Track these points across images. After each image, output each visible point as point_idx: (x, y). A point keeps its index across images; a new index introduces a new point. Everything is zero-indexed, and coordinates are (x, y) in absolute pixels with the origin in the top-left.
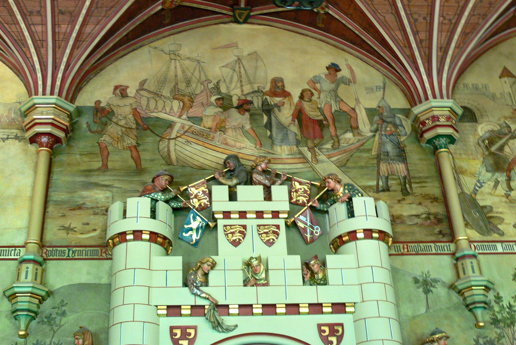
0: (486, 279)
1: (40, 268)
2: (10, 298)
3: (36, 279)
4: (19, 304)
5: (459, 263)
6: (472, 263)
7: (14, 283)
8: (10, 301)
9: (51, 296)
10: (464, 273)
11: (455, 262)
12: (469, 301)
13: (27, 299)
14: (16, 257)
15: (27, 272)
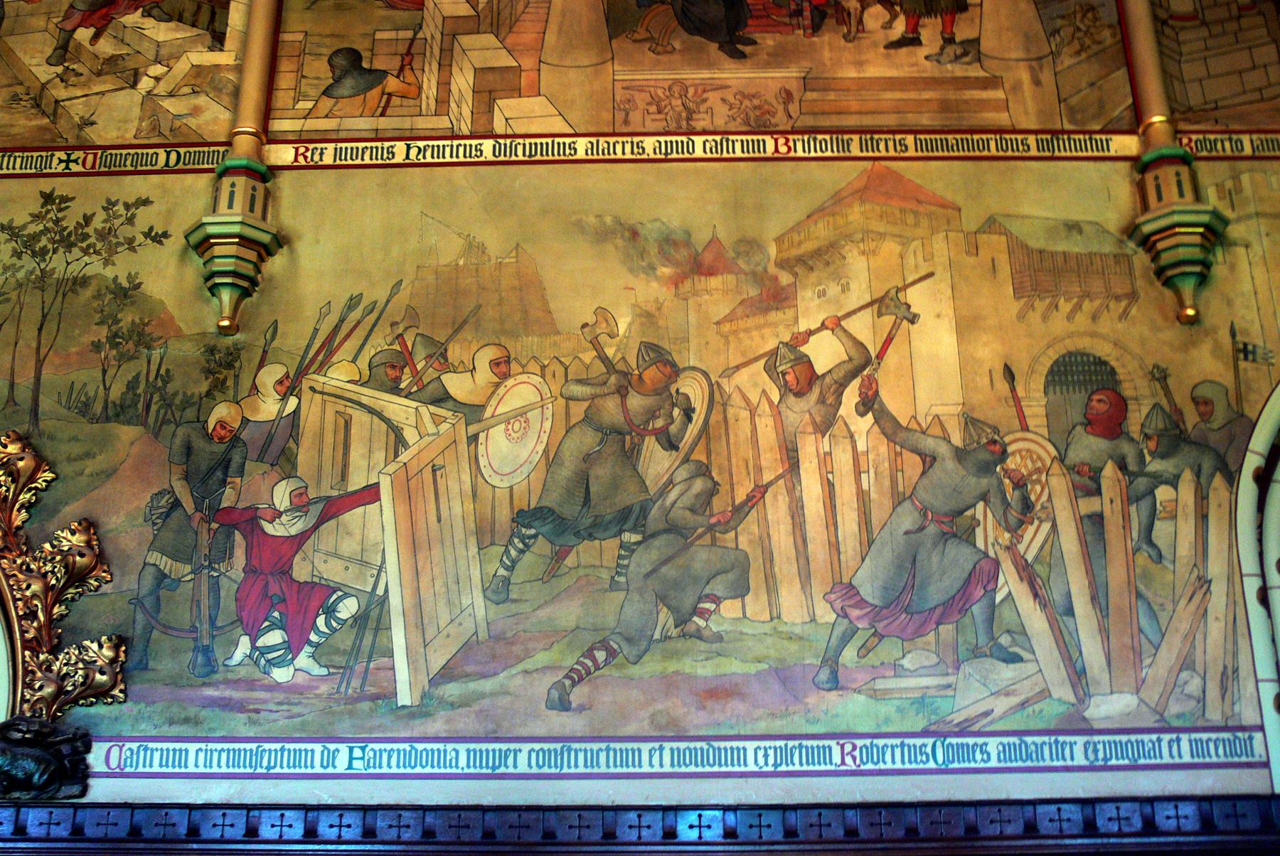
0: (1210, 208)
1: (260, 187)
2: (203, 248)
3: (252, 210)
4: (217, 260)
5: (1149, 177)
6: (1178, 174)
7: (206, 216)
8: (201, 255)
9: (285, 247)
10: (1160, 198)
11: (1138, 177)
12: (1166, 258)
13: (232, 250)
14: (211, 166)
15: (232, 194)
